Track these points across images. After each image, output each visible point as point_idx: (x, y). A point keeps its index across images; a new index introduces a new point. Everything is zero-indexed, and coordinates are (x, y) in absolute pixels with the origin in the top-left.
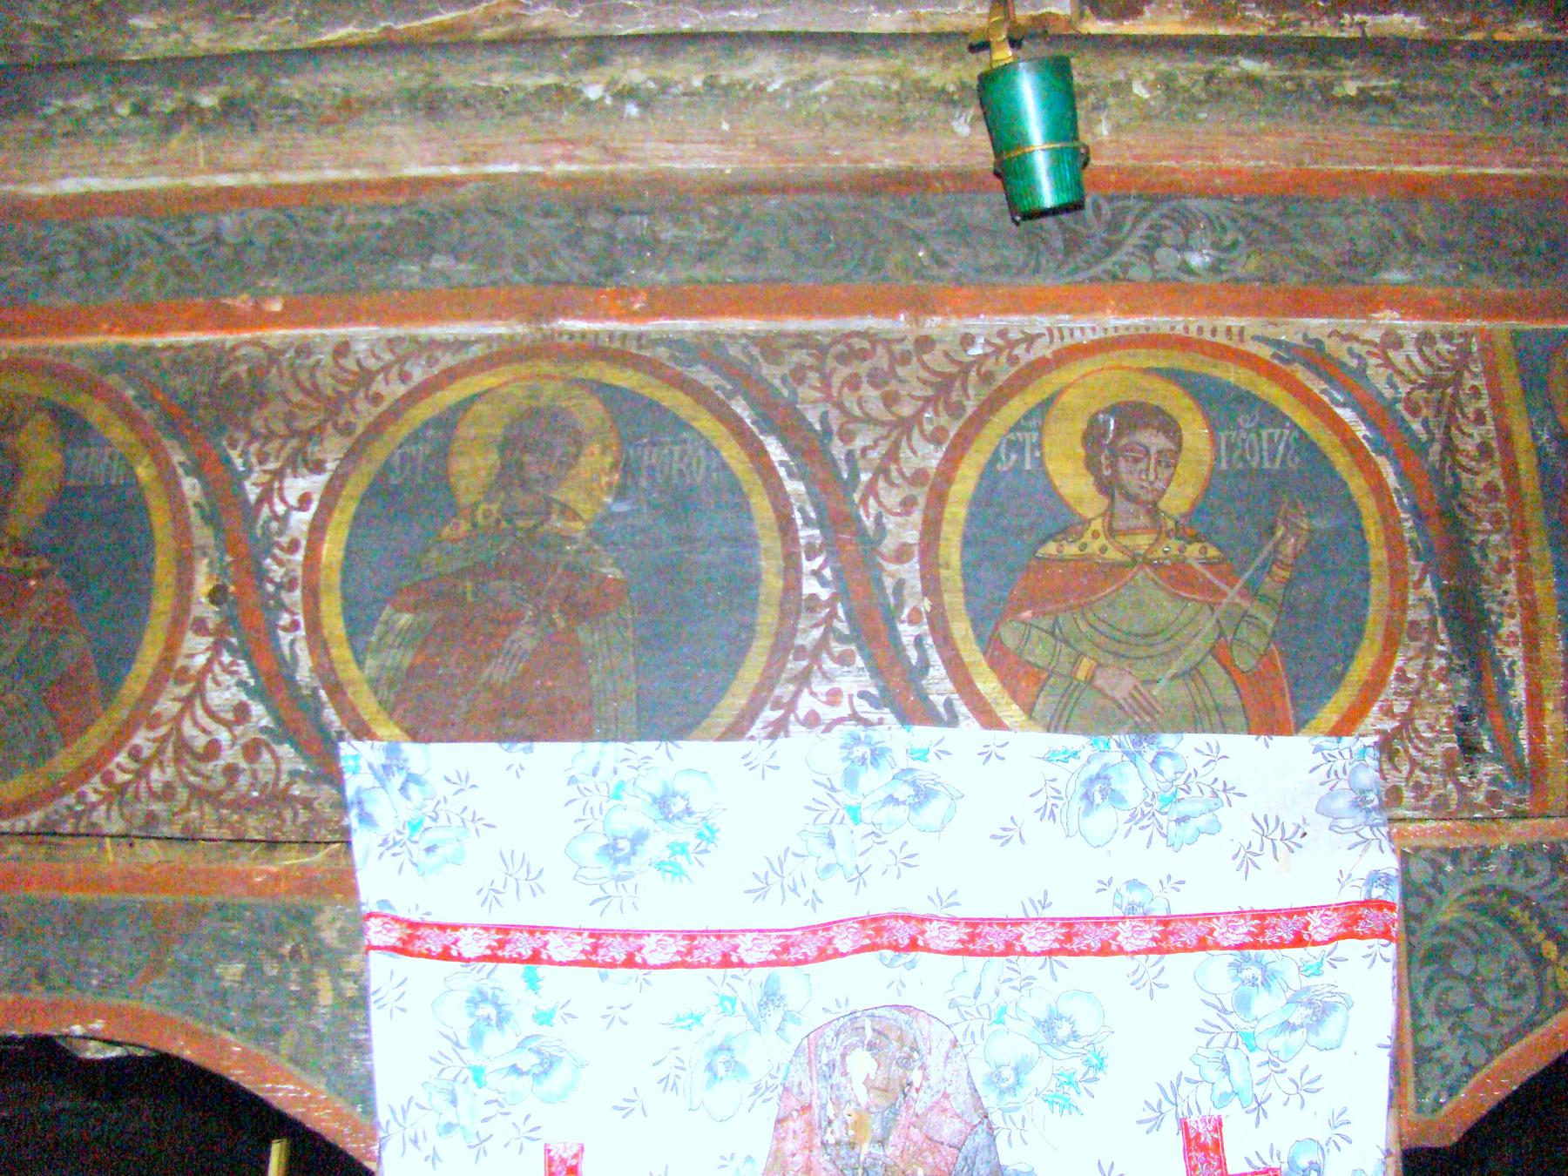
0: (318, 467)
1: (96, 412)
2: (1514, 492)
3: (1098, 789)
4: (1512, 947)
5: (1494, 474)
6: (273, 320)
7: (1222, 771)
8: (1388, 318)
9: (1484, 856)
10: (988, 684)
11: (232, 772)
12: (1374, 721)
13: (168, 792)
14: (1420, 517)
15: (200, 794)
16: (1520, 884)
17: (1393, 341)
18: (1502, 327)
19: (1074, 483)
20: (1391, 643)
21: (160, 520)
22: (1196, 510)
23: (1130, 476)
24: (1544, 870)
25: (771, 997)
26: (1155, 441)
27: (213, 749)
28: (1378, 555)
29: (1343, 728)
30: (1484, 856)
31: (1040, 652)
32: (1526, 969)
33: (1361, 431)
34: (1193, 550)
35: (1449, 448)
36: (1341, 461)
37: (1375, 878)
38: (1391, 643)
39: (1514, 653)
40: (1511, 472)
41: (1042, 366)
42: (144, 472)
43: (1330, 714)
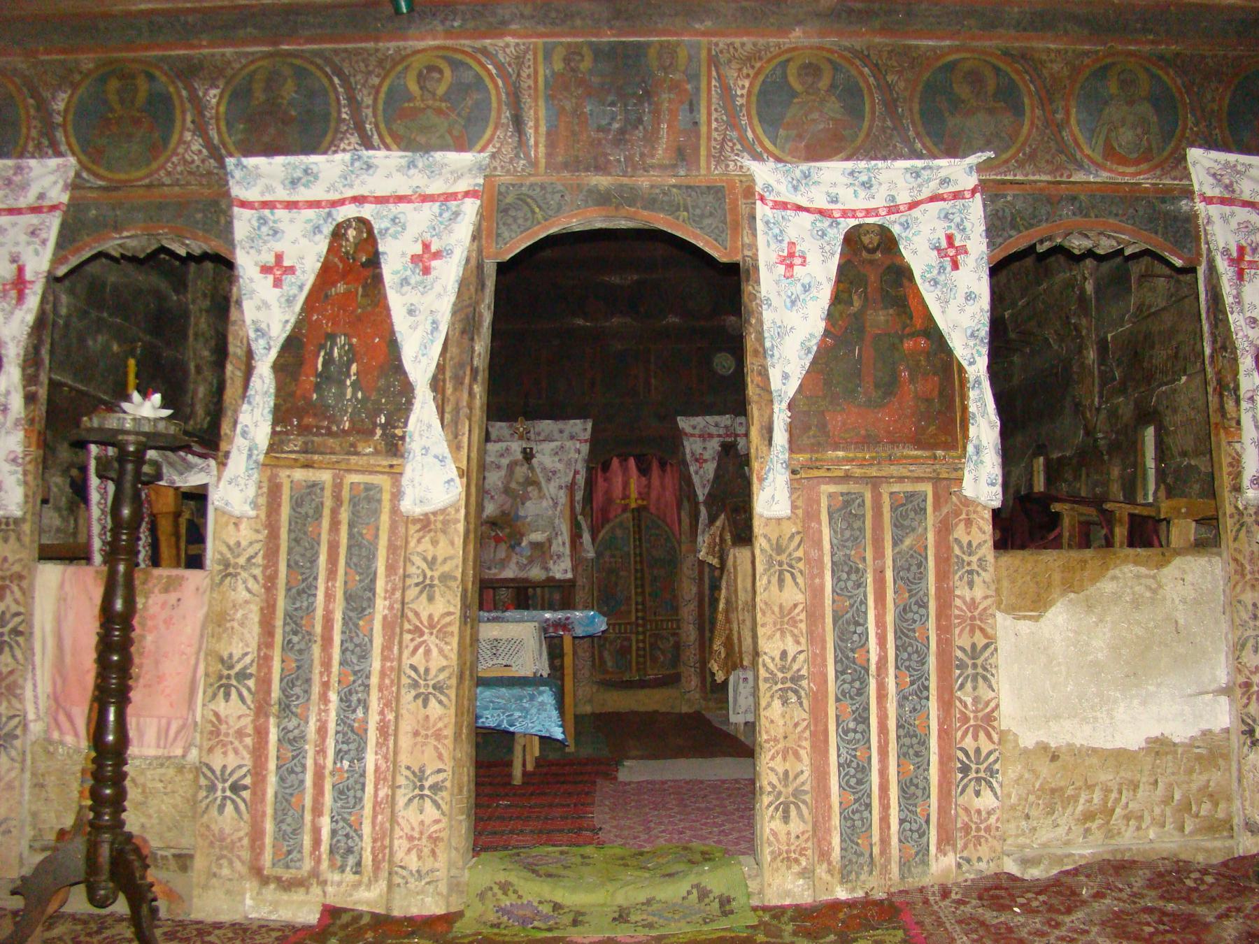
0: (217, 87)
1: (158, 73)
2: (536, 89)
3: (412, 164)
4: (526, 208)
5: (531, 82)
6: (205, 47)
7: (445, 161)
8: (509, 39)
9: (522, 185)
10: (389, 140)
11: (198, 167)
12: (491, 149)
13: (182, 173)
14: (508, 94)
15: (190, 173)
16: (530, 193)
17: (507, 45)
18: (540, 41)
19: (413, 87)
20: (496, 128)
21: (177, 102)
22: (446, 93)
23: (428, 85)
24: (538, 189)
25: (329, 214)
26: (436, 75)
27: (193, 161)
28: (494, 105)
29: (480, 151)
30: (522, 185)
31: (402, 131)
32: (529, 215)
33: (494, 71)
34: (444, 105)
35: (519, 75)
36: (487, 80)
37: (478, 185)
38: (496, 128)
39: (531, 131)
40: (536, 82)
41: (408, 56)
42: (172, 89)
43: (478, 147)
